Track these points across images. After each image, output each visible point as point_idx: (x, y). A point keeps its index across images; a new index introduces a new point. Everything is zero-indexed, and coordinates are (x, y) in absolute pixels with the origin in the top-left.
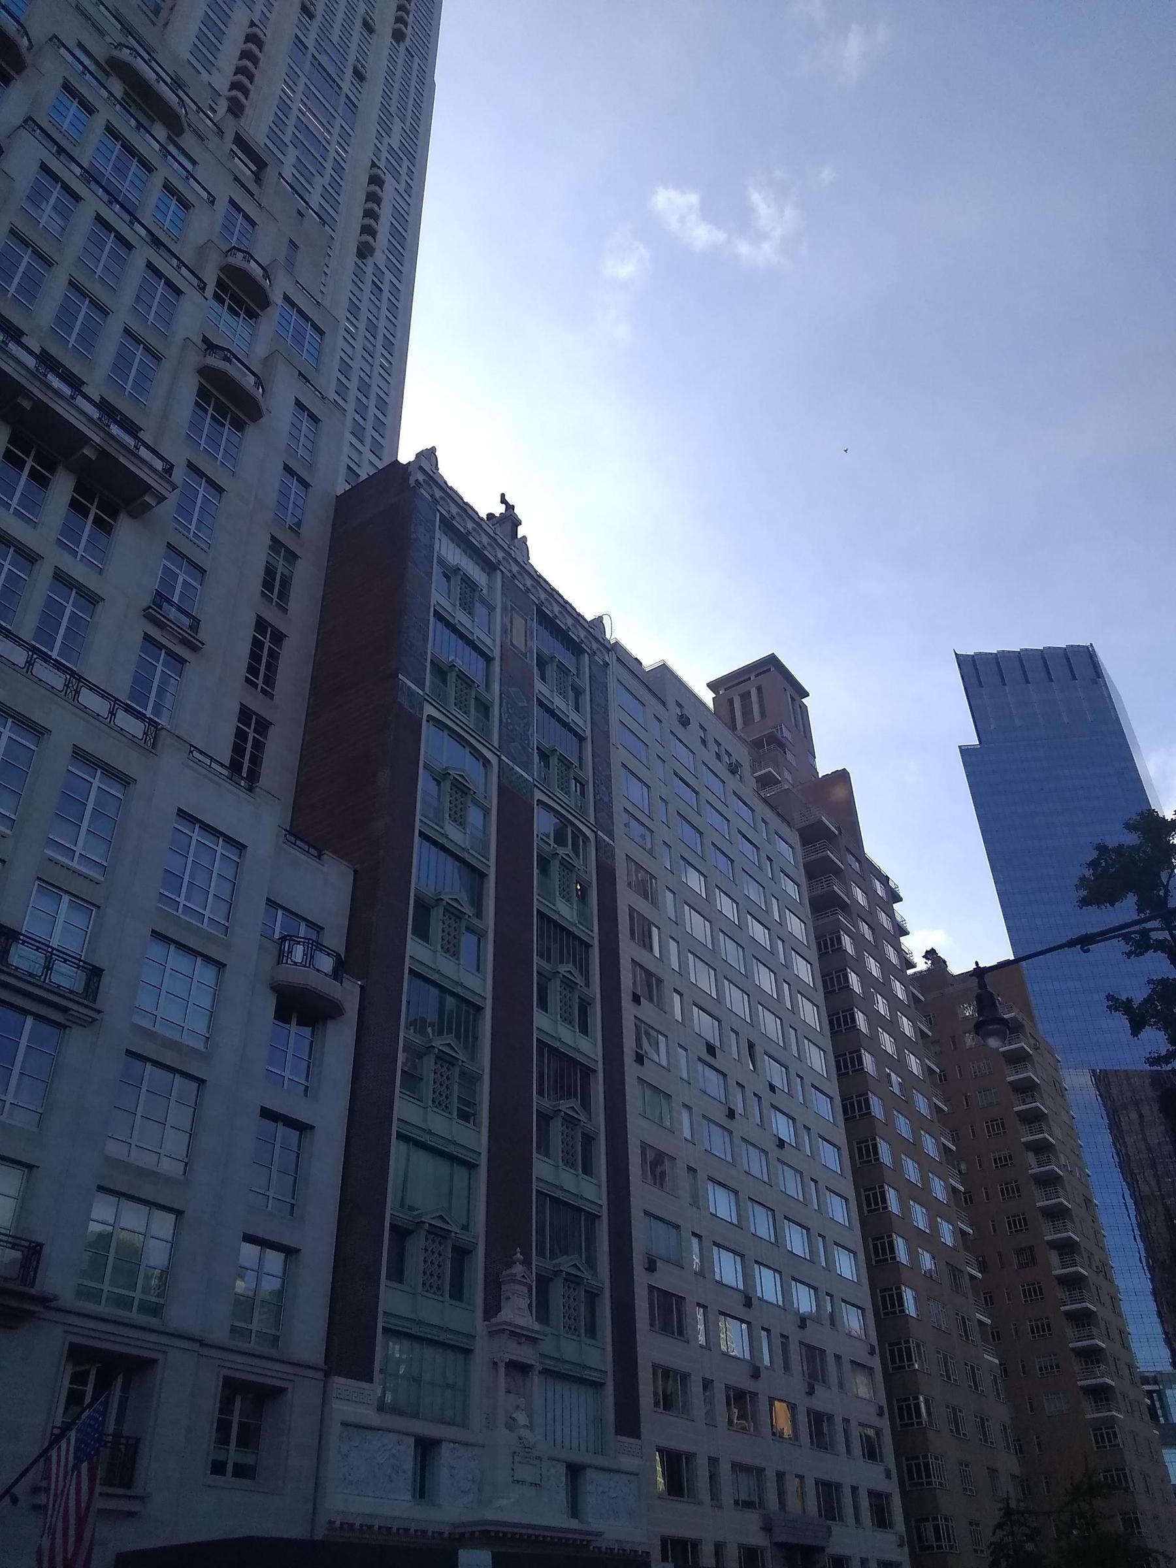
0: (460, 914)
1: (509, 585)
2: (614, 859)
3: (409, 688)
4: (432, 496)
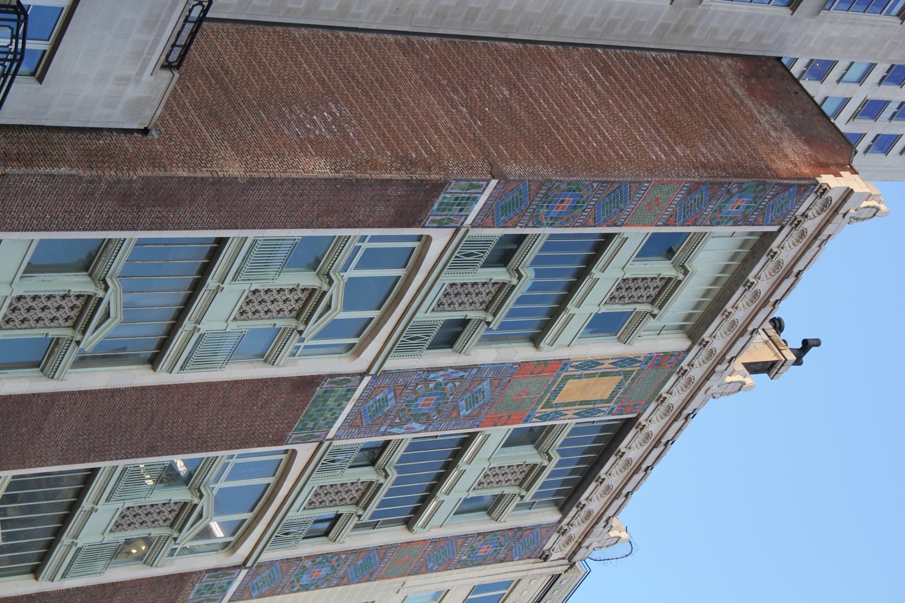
0: (80, 326)
1: (666, 363)
3: (476, 200)
4: (804, 215)
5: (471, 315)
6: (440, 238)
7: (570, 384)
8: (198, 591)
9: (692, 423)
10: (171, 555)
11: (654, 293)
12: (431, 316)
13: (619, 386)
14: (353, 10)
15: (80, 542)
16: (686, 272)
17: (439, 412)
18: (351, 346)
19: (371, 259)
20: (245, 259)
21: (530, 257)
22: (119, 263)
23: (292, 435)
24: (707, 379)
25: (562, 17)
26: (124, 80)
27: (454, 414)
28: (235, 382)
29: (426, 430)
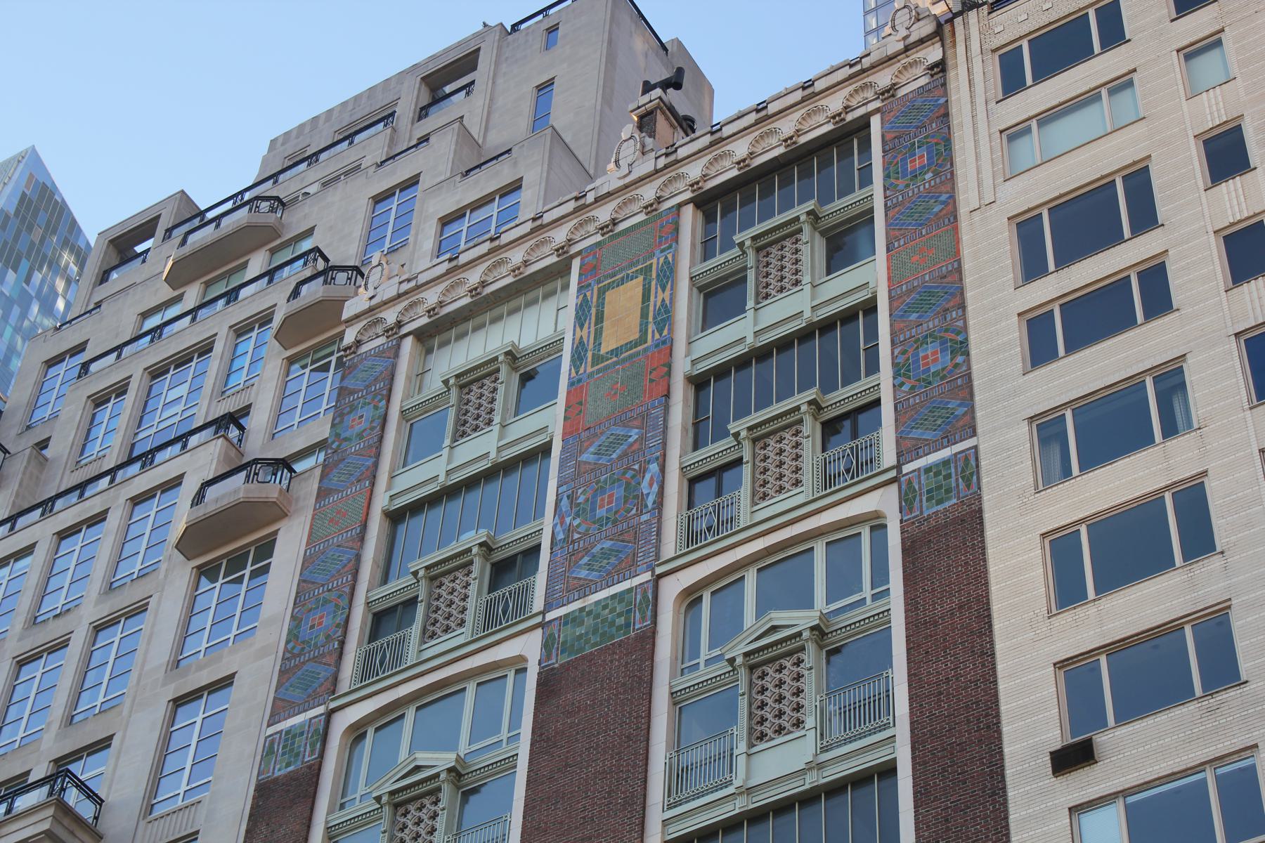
8: (939, 502)
16: (446, 382)
24: (609, 194)
27: (636, 447)
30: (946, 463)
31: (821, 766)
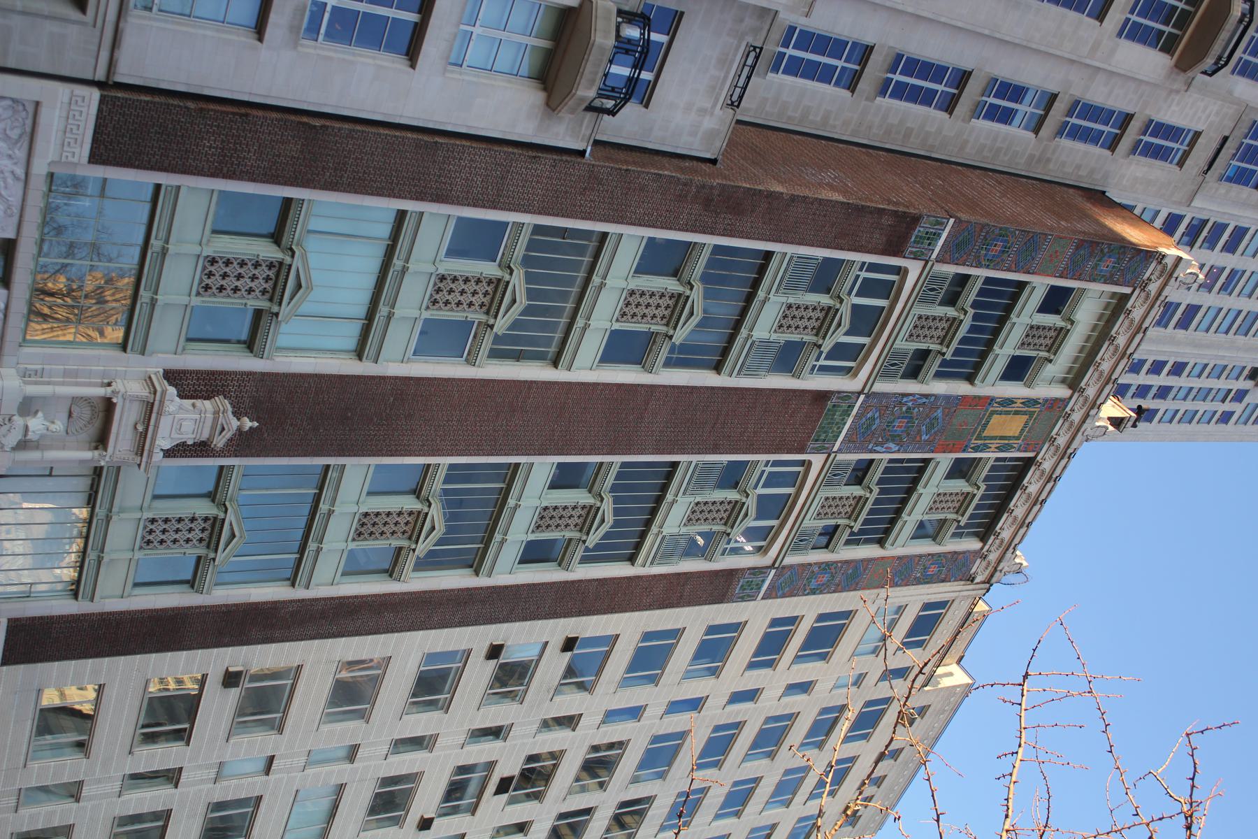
1: (1055, 406)
2: (743, 599)
3: (939, 236)
4: (1149, 279)
5: (840, 522)
6: (817, 460)
7: (995, 419)
9: (1059, 484)
10: (723, 554)
11: (1049, 342)
12: (812, 523)
13: (1026, 423)
14: (831, 122)
15: (666, 531)
16: (1072, 323)
17: (908, 435)
18: (761, 547)
19: (773, 480)
20: (656, 554)
21: (876, 478)
22: (699, 266)
23: (811, 445)
24: (1084, 422)
25: (967, 142)
26: (703, 112)
28: (774, 390)
29: (898, 451)
30: (760, 588)
31: (657, 535)
